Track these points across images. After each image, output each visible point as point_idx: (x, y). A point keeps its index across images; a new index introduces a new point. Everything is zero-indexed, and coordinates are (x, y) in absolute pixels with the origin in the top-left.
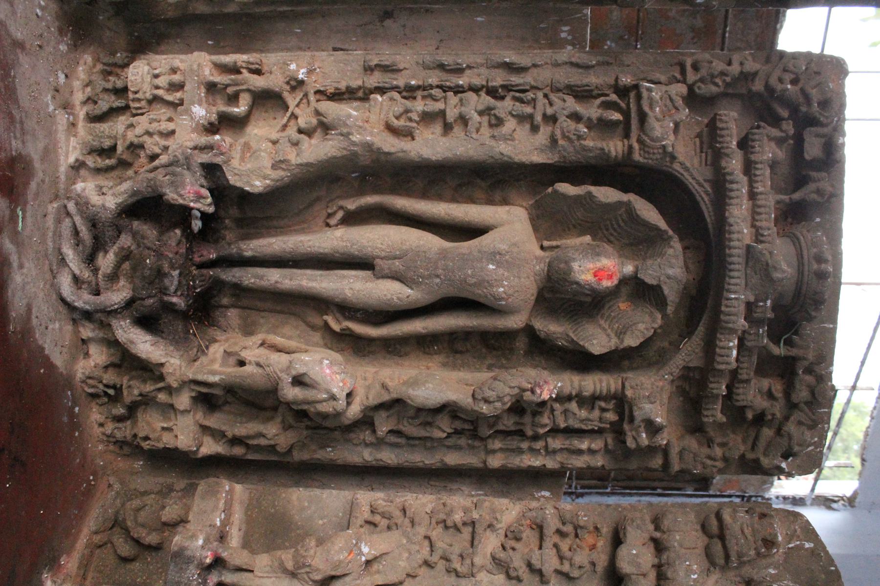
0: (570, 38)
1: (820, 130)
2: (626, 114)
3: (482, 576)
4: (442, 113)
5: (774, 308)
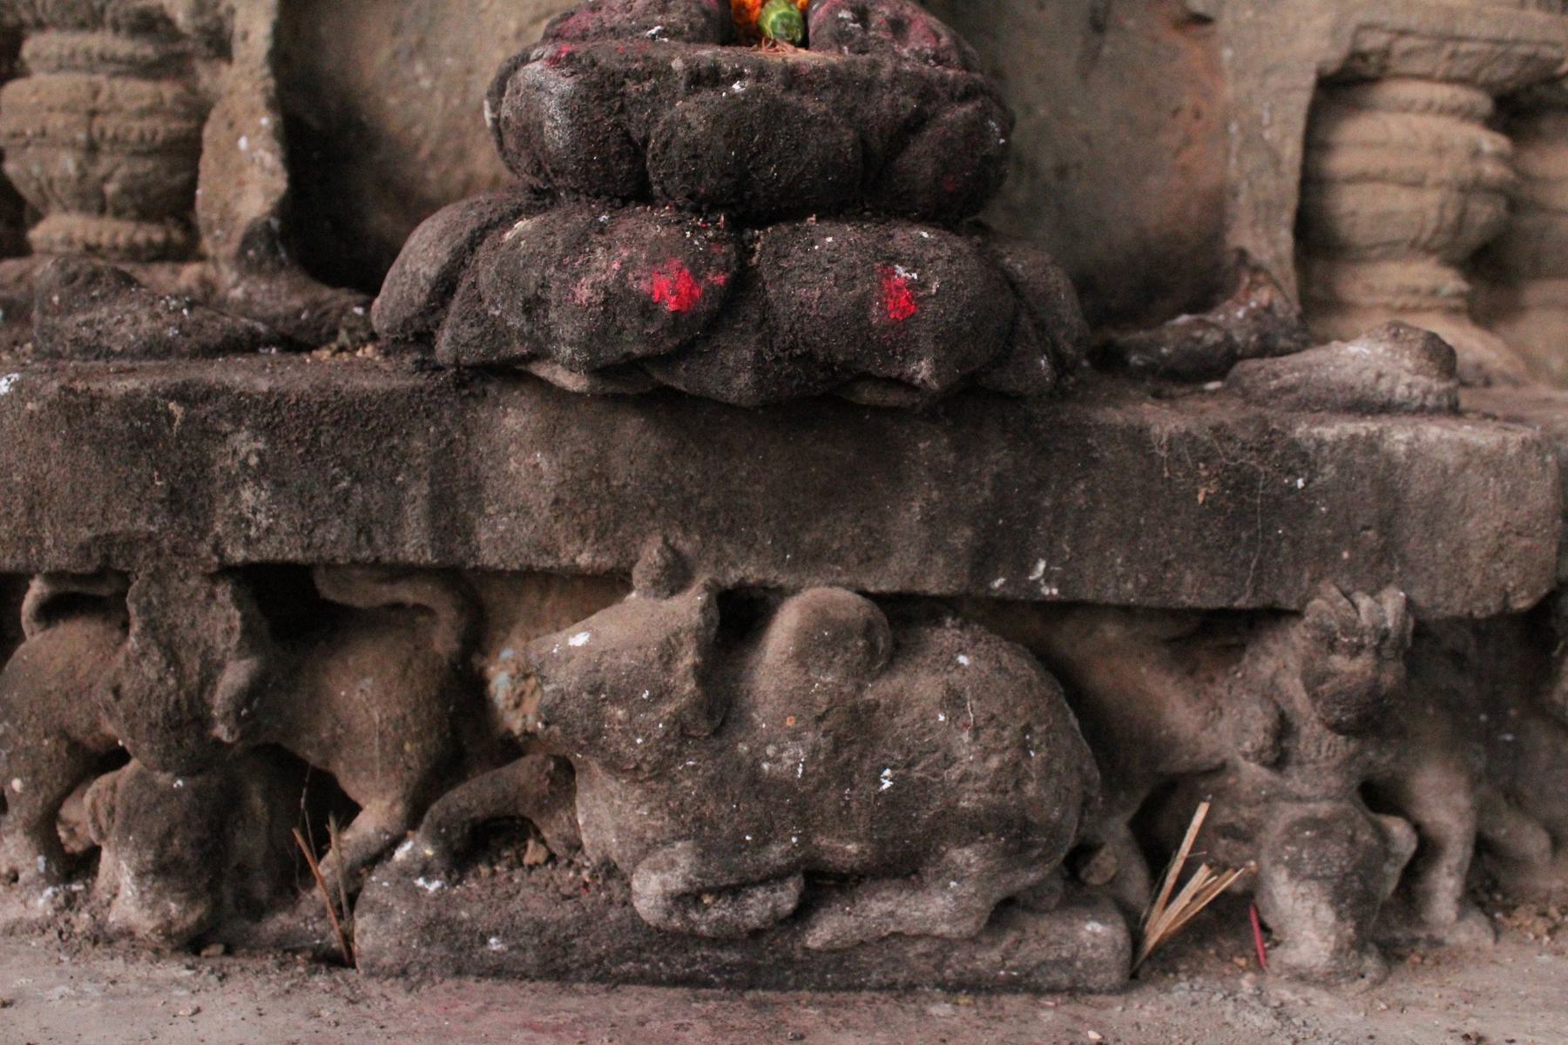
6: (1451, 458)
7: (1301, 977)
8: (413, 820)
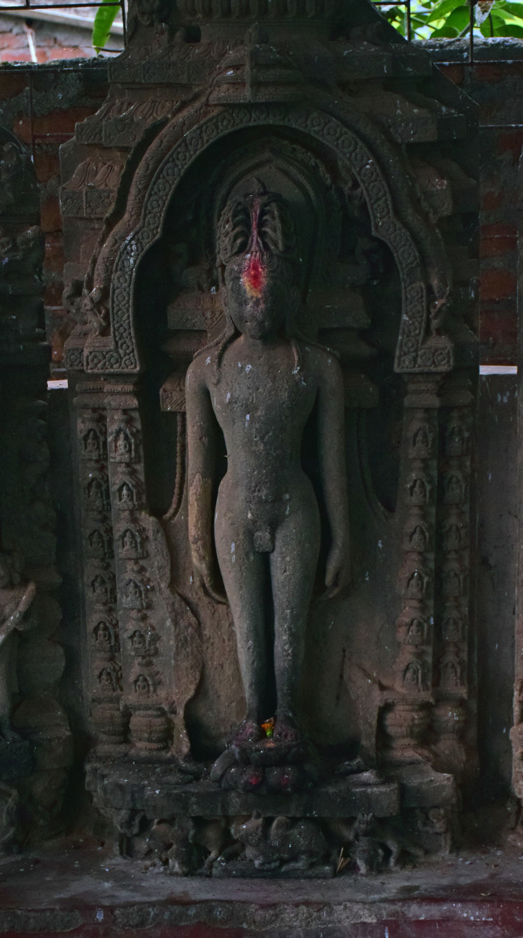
0: (508, 394)
6: (378, 793)
7: (362, 875)
8: (219, 854)
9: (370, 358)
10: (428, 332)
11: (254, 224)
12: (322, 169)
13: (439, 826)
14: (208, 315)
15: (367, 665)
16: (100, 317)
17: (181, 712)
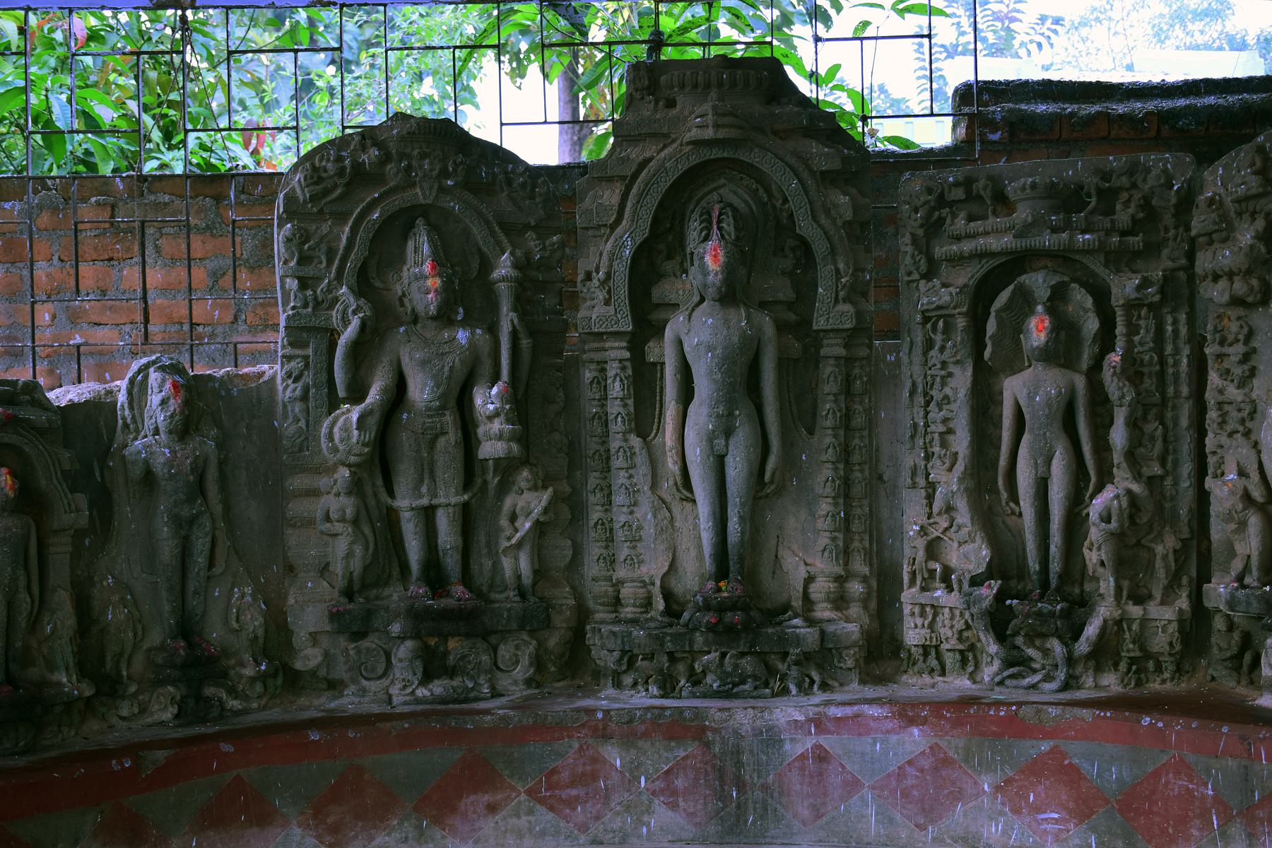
1: (946, 189)
2: (940, 317)
3: (1254, 396)
4: (941, 434)
5: (1056, 213)
9: (797, 325)
10: (837, 301)
11: (715, 221)
12: (761, 191)
13: (850, 663)
14: (681, 292)
15: (795, 547)
16: (604, 292)
17: (658, 583)
